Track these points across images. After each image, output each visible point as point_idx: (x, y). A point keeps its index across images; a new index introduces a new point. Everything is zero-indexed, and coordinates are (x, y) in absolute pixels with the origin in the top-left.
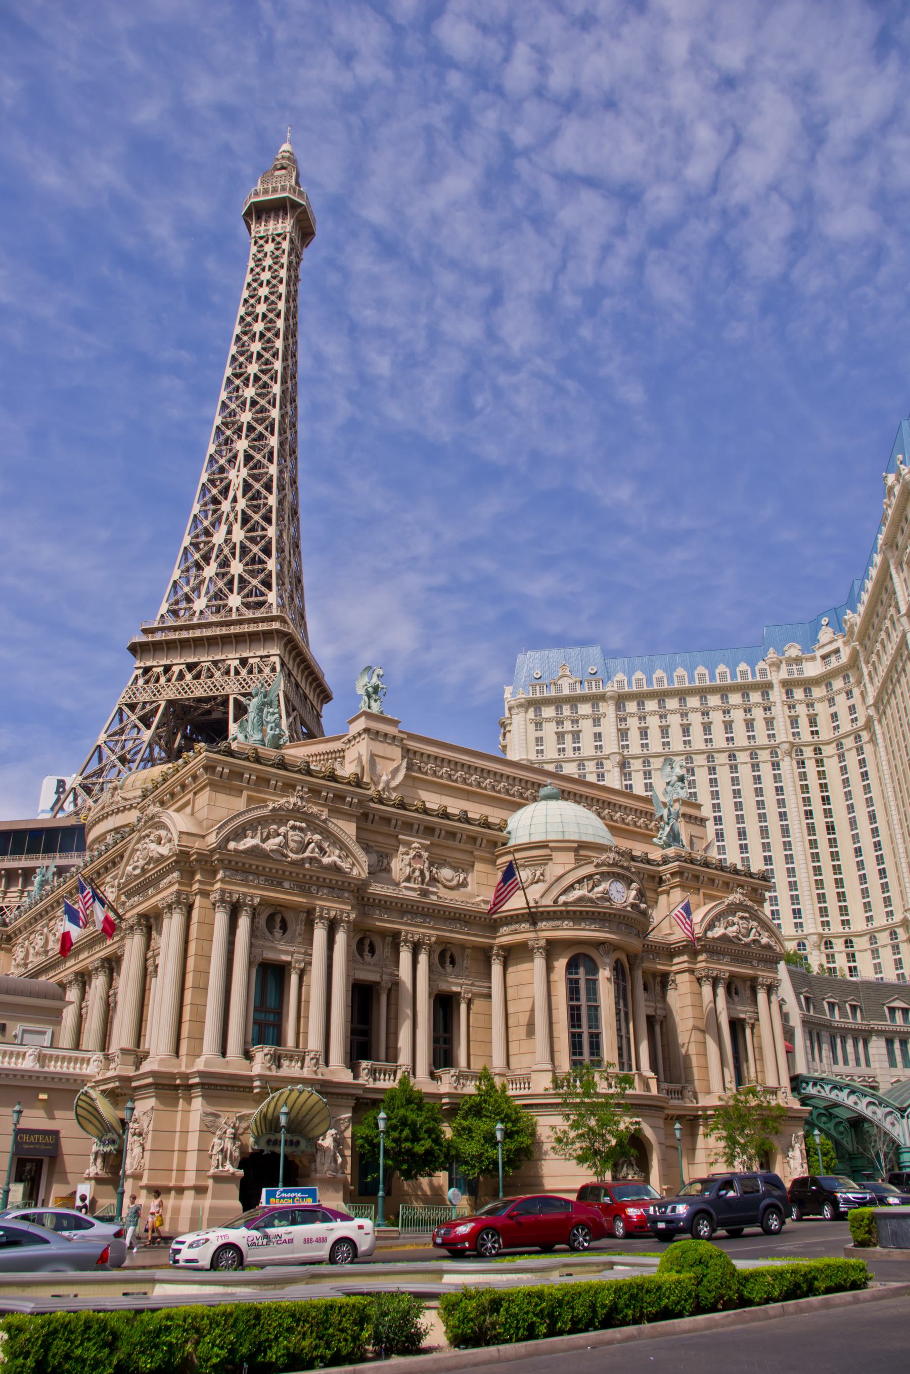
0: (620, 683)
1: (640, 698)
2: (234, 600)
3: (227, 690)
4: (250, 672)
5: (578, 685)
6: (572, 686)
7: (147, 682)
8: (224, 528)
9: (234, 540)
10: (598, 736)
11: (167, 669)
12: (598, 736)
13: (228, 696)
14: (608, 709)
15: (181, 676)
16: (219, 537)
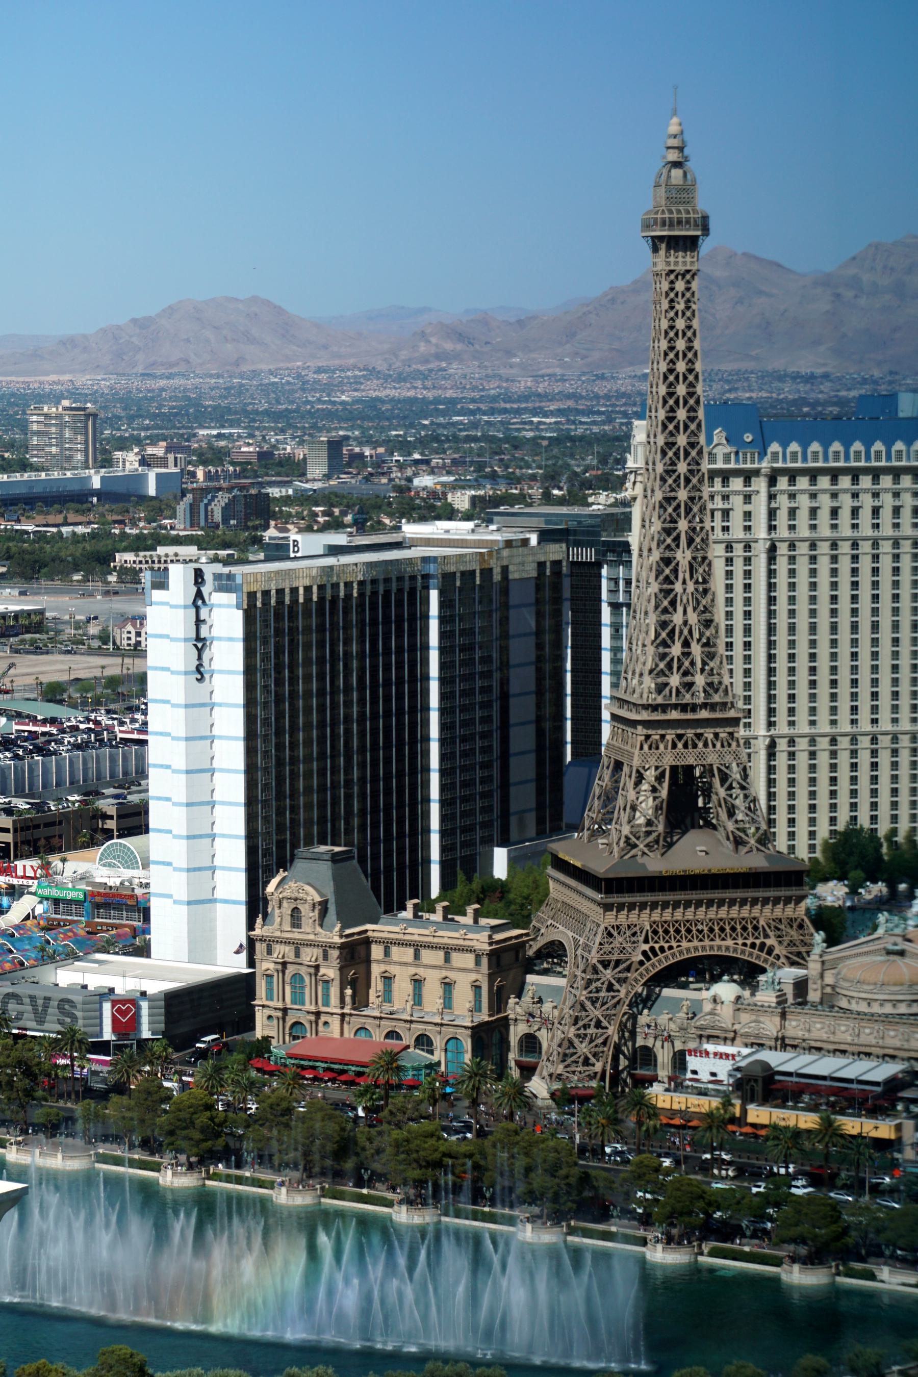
0: (775, 456)
1: (792, 475)
2: (700, 680)
3: (709, 760)
4: (723, 746)
5: (733, 456)
6: (727, 459)
7: (650, 748)
8: (680, 609)
9: (690, 622)
10: (748, 515)
11: (663, 737)
12: (748, 515)
13: (711, 765)
14: (760, 485)
15: (674, 746)
16: (677, 618)
